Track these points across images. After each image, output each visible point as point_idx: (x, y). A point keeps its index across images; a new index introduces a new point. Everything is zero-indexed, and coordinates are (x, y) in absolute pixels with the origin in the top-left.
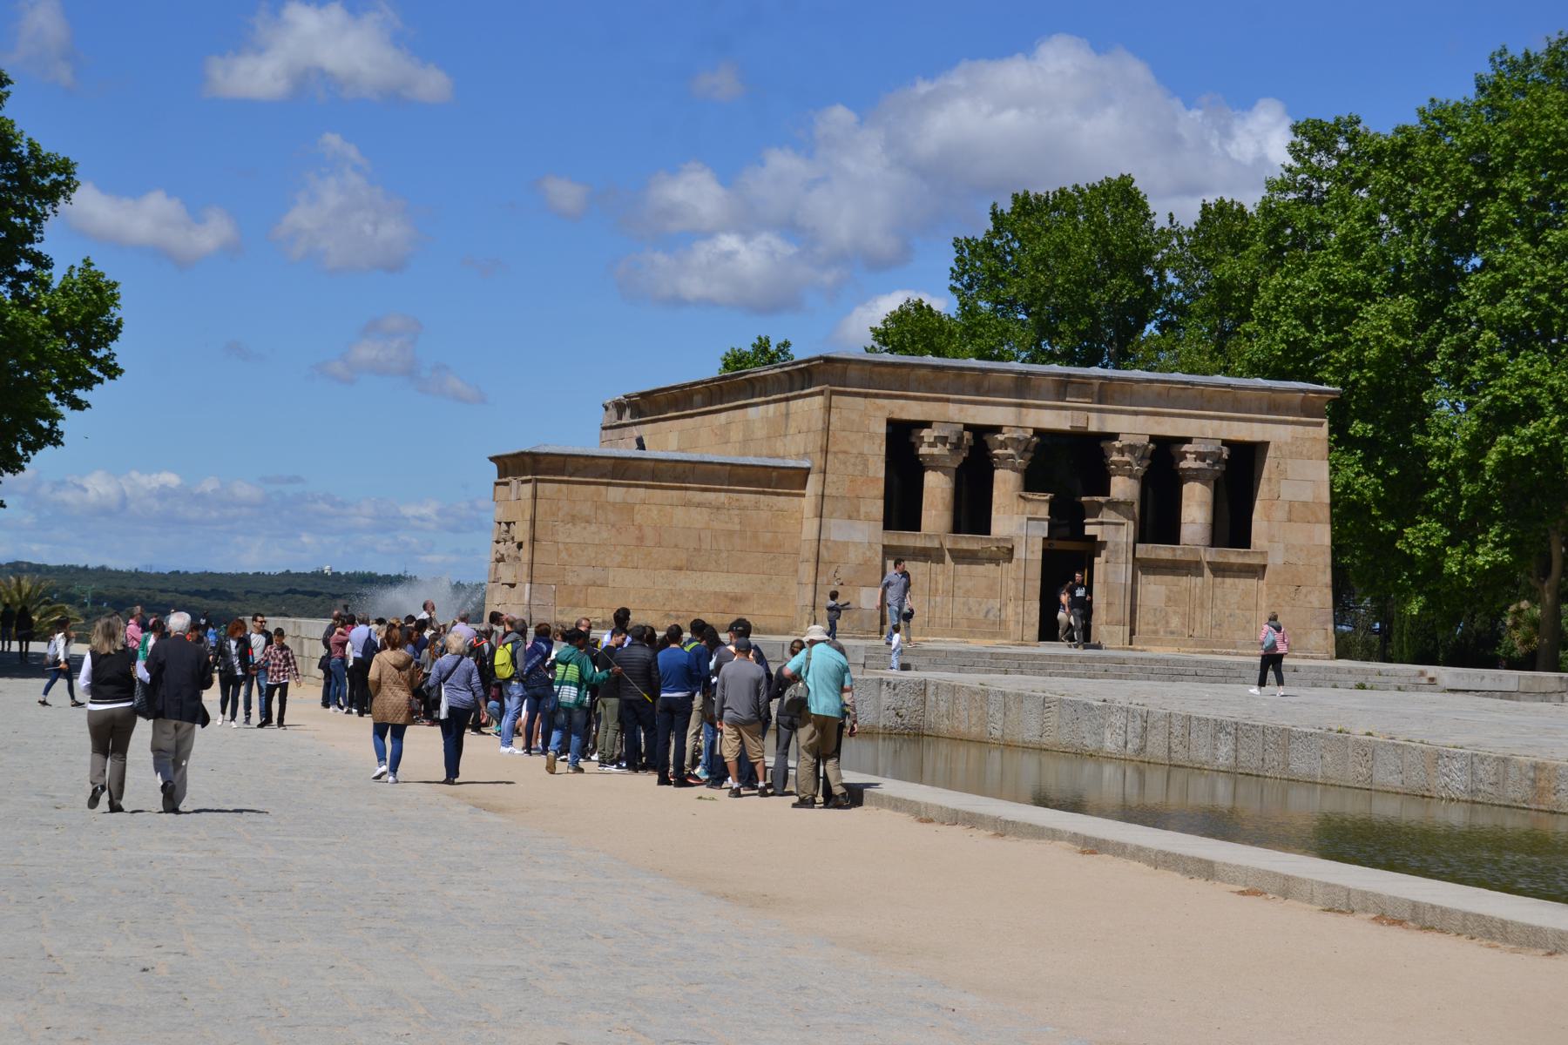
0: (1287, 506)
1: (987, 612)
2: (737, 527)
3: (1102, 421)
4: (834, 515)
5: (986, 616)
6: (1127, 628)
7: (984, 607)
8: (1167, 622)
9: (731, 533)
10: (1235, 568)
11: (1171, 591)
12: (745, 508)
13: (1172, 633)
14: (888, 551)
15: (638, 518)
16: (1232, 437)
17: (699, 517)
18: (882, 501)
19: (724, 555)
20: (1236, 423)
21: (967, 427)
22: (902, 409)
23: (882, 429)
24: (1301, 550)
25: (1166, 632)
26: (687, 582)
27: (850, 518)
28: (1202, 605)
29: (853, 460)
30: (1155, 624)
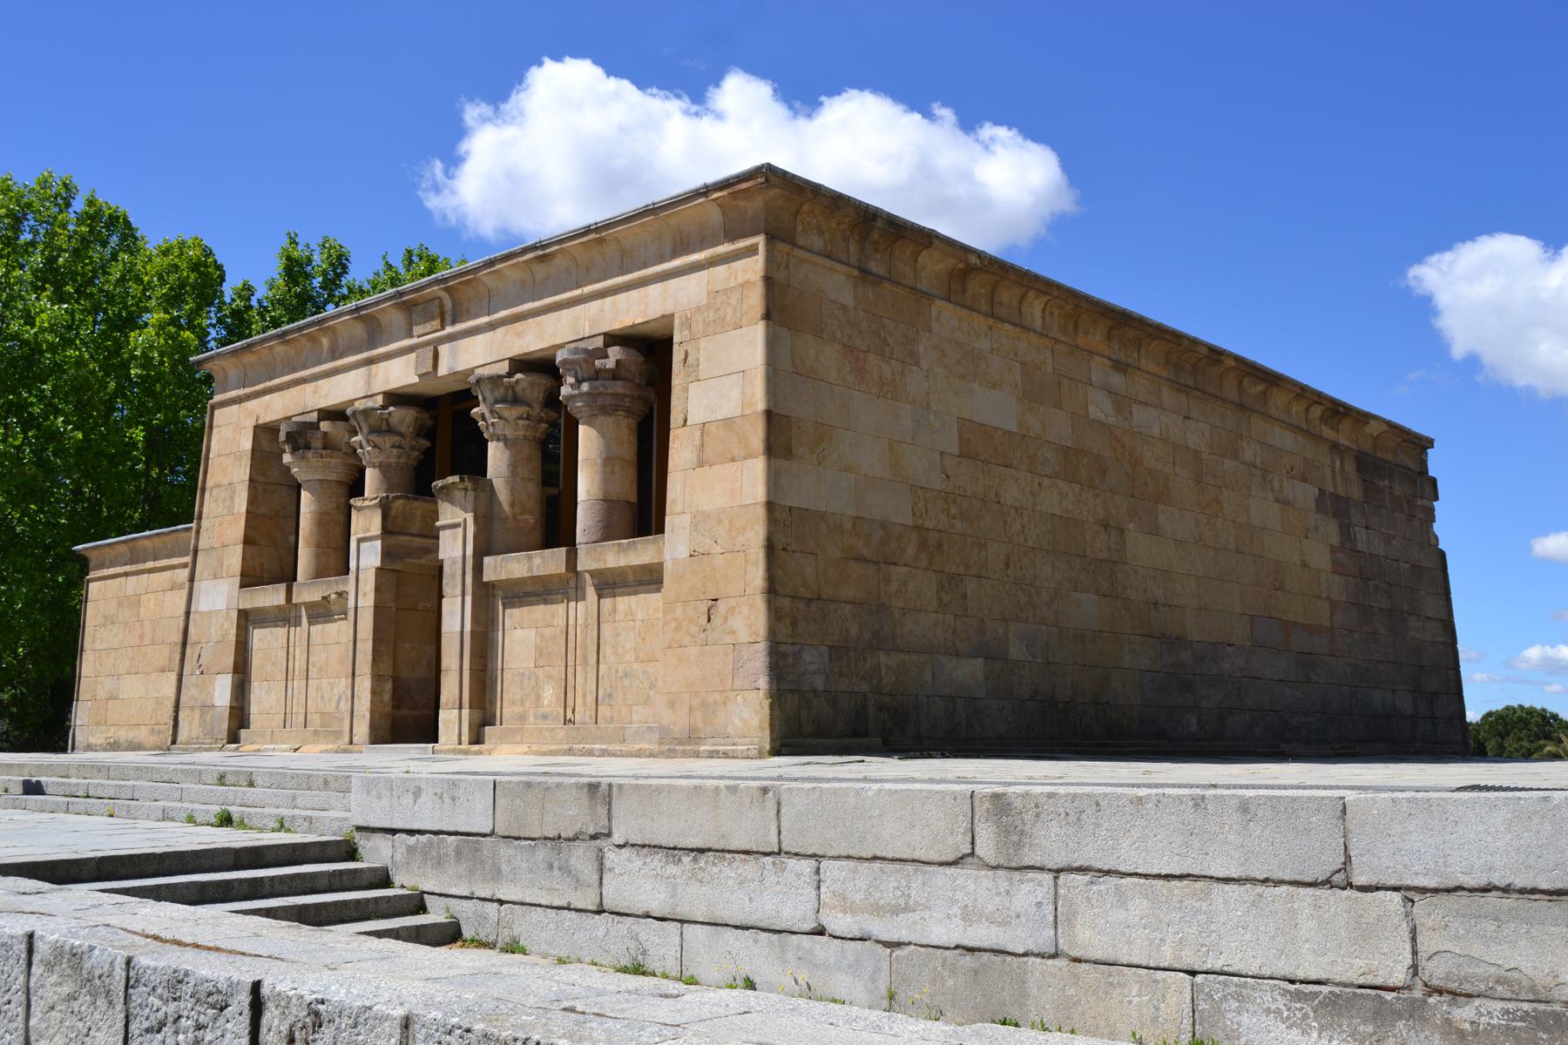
1: (339, 701)
3: (454, 355)
5: (337, 708)
8: (538, 697)
10: (631, 578)
11: (542, 637)
13: (545, 717)
20: (623, 296)
24: (720, 521)
27: (215, 577)
30: (522, 703)
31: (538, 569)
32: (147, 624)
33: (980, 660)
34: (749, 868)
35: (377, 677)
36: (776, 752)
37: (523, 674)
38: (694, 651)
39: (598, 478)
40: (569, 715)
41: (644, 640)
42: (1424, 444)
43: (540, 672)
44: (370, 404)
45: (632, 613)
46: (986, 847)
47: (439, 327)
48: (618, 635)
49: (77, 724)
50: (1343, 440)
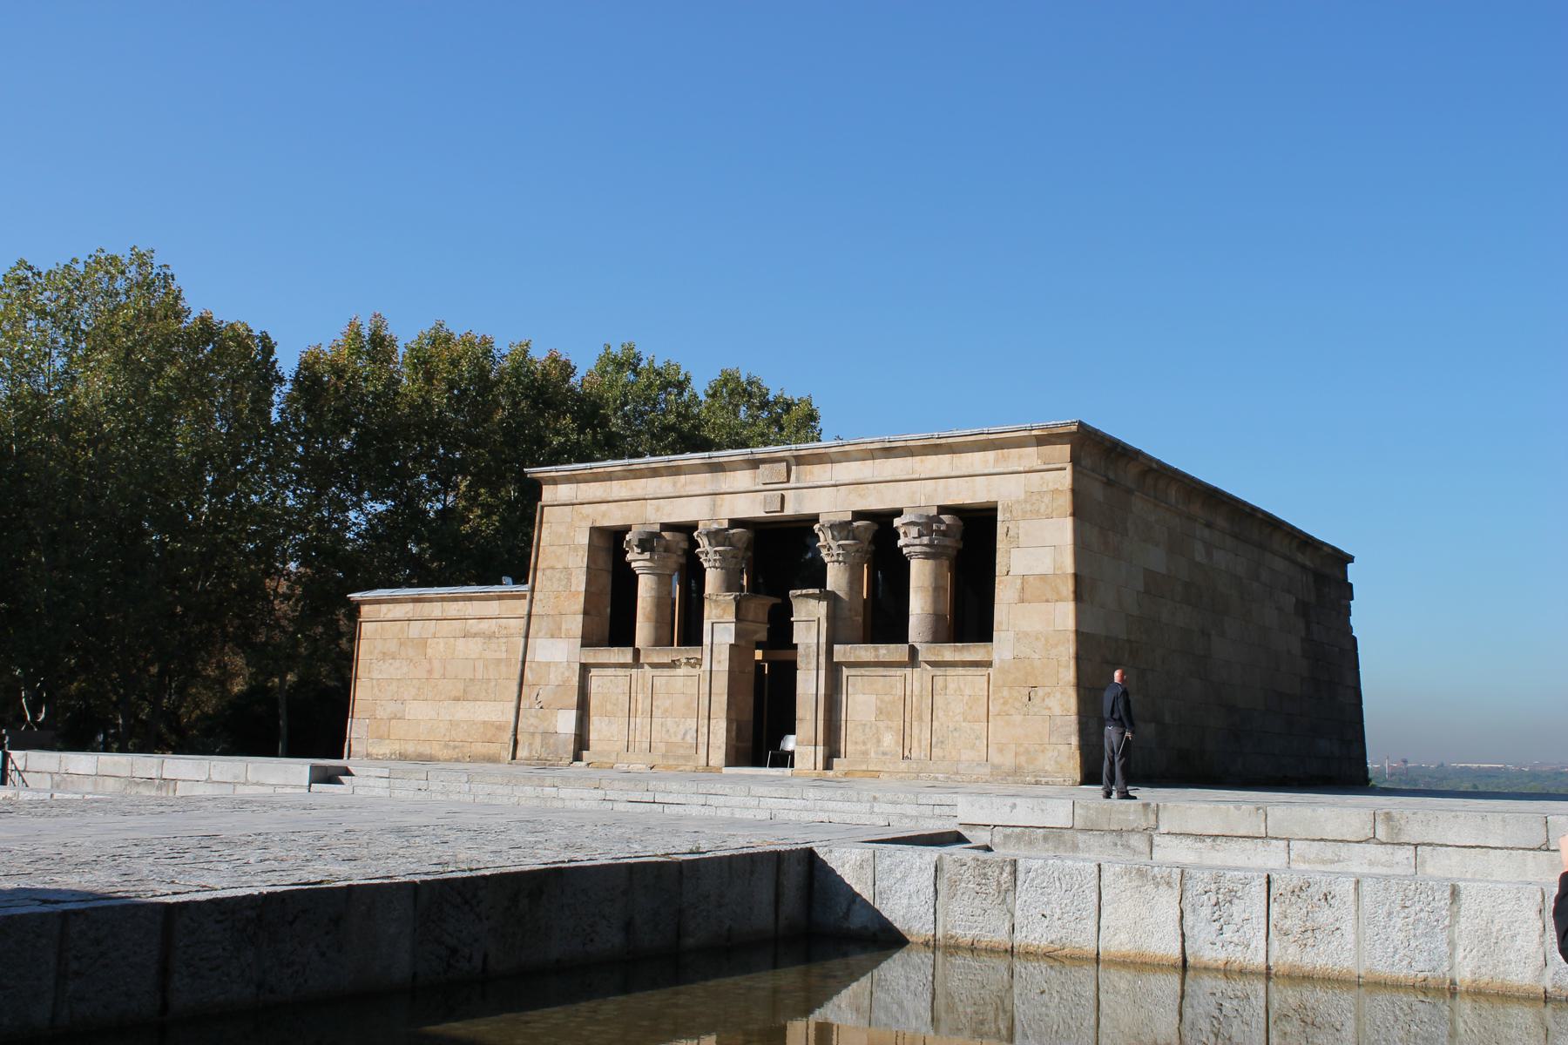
0: (1019, 581)
1: (685, 734)
2: (504, 656)
3: (799, 500)
4: (540, 634)
5: (683, 739)
6: (820, 749)
7: (682, 729)
8: (879, 741)
9: (499, 661)
11: (882, 701)
12: (511, 635)
13: (884, 754)
14: (585, 668)
15: (429, 651)
16: (949, 502)
17: (473, 647)
18: (580, 618)
19: (493, 683)
21: (666, 527)
22: (604, 515)
23: (584, 539)
24: (1037, 639)
25: (876, 753)
26: (463, 712)
27: (552, 637)
28: (921, 719)
29: (558, 575)
30: (864, 743)
31: (883, 657)
32: (436, 664)
33: (1153, 725)
34: (1249, 844)
35: (729, 721)
36: (1082, 783)
37: (865, 725)
38: (1018, 718)
39: (929, 600)
40: (907, 753)
41: (971, 708)
42: (1344, 559)
43: (880, 724)
44: (715, 526)
45: (960, 689)
46: (1381, 834)
47: (786, 480)
48: (949, 703)
49: (352, 736)
50: (1308, 563)
